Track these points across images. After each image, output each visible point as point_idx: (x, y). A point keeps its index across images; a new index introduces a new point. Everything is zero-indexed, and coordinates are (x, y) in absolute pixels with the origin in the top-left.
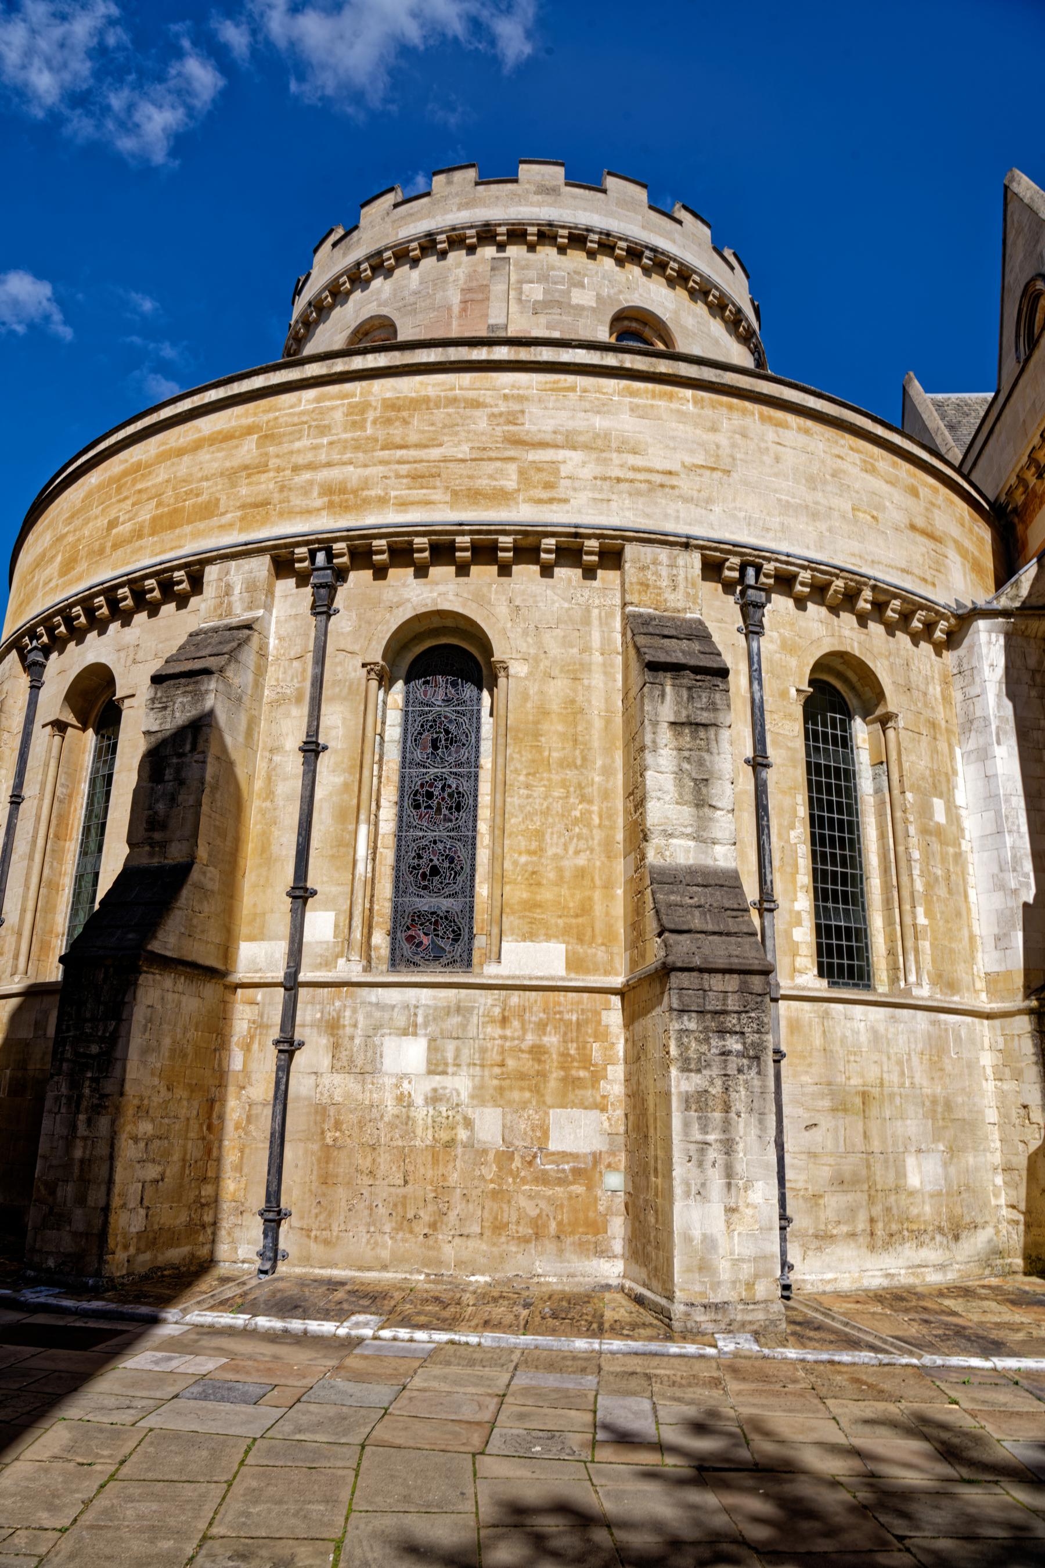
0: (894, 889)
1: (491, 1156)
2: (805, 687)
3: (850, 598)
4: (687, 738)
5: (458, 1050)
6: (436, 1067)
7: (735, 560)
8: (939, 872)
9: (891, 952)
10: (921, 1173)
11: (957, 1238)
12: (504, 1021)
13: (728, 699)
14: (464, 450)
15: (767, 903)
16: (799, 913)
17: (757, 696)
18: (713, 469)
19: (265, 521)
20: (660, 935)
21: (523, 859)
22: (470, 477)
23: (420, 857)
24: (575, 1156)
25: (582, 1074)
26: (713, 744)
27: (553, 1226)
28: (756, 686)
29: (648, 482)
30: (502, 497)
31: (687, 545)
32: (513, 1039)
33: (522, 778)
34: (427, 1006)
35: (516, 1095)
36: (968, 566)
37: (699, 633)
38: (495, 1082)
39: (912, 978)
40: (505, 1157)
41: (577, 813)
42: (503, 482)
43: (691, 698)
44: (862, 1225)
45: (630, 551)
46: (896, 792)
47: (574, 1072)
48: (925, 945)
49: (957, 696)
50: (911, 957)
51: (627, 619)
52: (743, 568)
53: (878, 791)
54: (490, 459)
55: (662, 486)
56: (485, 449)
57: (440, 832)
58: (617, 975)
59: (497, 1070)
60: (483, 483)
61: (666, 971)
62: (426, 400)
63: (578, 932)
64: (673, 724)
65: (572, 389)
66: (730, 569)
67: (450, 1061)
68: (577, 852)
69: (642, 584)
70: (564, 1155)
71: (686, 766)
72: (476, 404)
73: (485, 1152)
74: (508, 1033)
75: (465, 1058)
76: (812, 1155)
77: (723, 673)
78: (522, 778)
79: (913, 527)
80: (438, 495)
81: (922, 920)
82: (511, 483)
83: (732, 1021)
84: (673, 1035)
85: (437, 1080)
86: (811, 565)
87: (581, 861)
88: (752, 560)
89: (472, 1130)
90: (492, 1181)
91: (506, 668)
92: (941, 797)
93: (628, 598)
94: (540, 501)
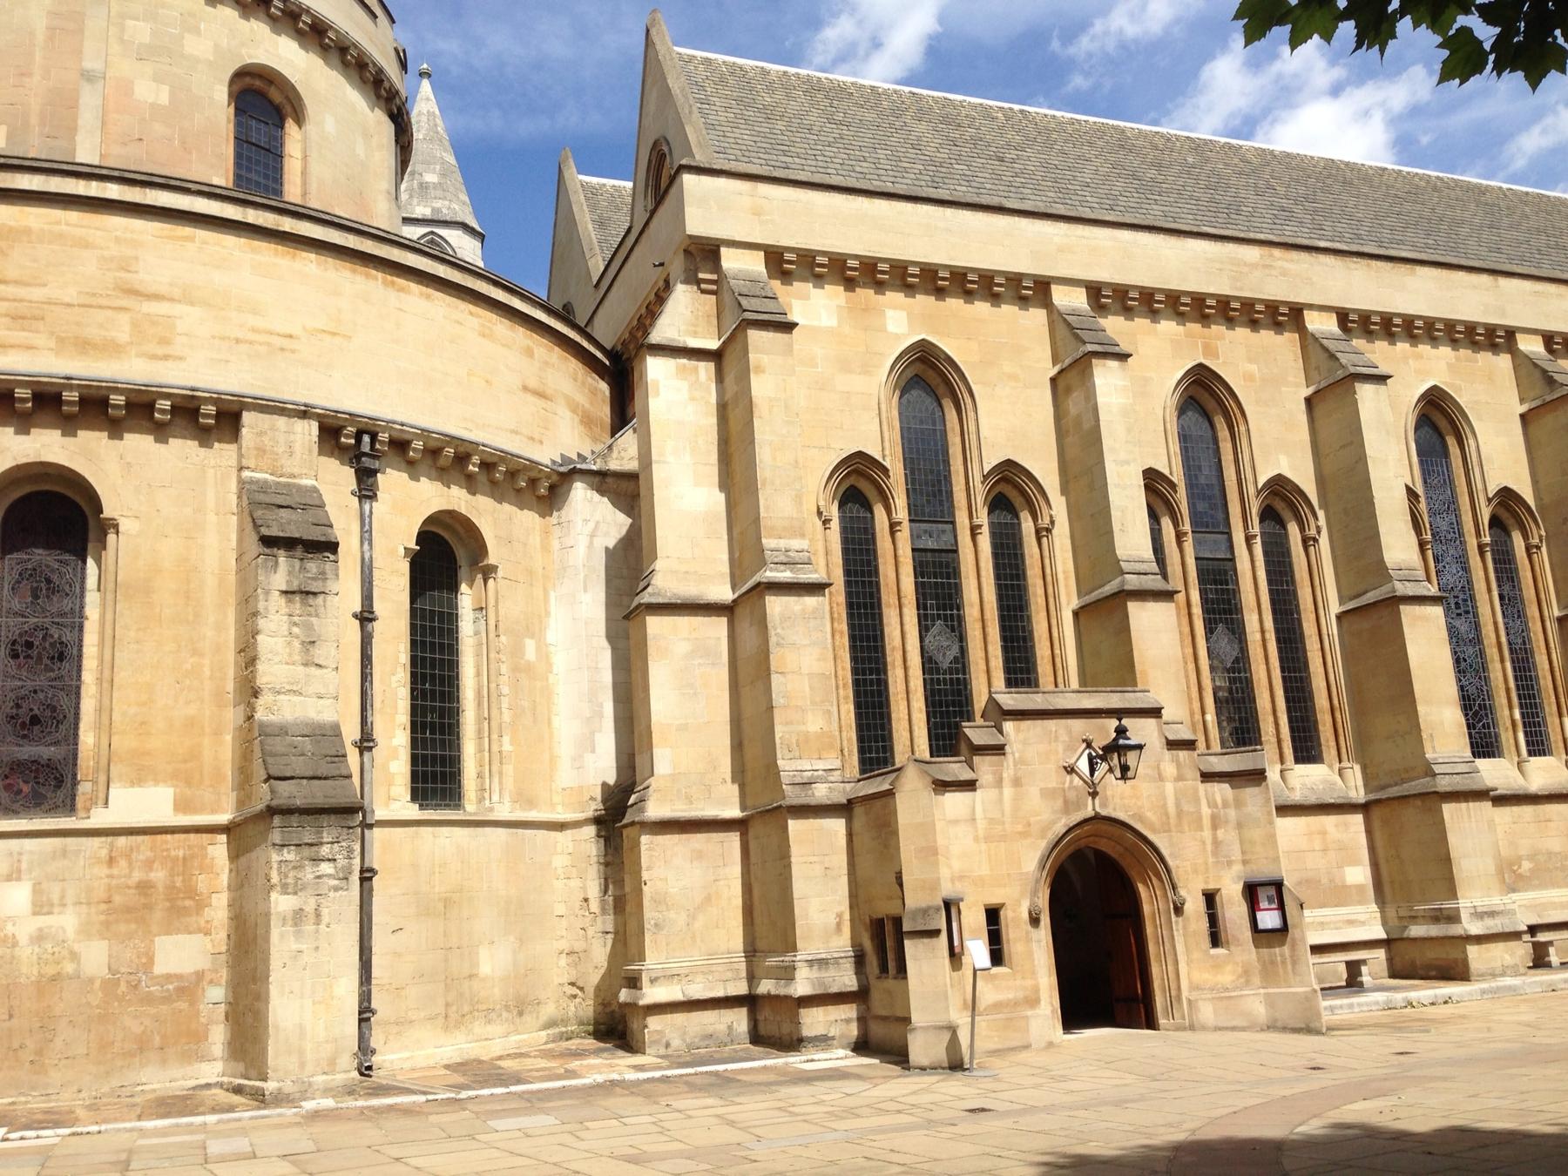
0: (485, 719)
1: (97, 984)
2: (413, 545)
3: (462, 459)
4: (297, 606)
5: (63, 891)
6: (41, 906)
8: (526, 704)
9: (480, 776)
10: (493, 962)
11: (521, 1014)
12: (111, 861)
13: (337, 569)
14: (70, 295)
15: (366, 743)
16: (396, 749)
17: (367, 556)
18: (334, 334)
20: (266, 781)
21: (132, 711)
22: (78, 324)
23: (18, 706)
24: (179, 977)
25: (188, 903)
26: (322, 610)
27: (157, 1040)
28: (366, 546)
29: (269, 344)
30: (112, 349)
31: (304, 413)
32: (119, 877)
33: (132, 634)
34: (31, 852)
35: (123, 928)
36: (577, 419)
37: (312, 503)
38: (103, 917)
39: (495, 798)
40: (109, 986)
41: (188, 666)
42: (114, 334)
43: (303, 569)
44: (441, 1009)
45: (247, 417)
46: (492, 635)
47: (180, 903)
48: (509, 769)
49: (555, 544)
50: (496, 780)
51: (241, 482)
52: (358, 436)
53: (477, 633)
54: (100, 307)
55: (282, 349)
56: (94, 295)
57: (41, 681)
58: (224, 812)
59: (103, 907)
60: (92, 332)
61: (272, 811)
62: (28, 231)
63: (184, 775)
64: (285, 592)
65: (191, 239)
66: (347, 436)
67: (56, 901)
68: (188, 702)
69: (258, 449)
70: (169, 978)
71: (296, 630)
72: (86, 245)
73: (91, 980)
74: (115, 871)
75: (69, 900)
76: (397, 954)
77: (333, 547)
78: (132, 634)
79: (525, 388)
80: (40, 340)
81: (507, 747)
82: (123, 334)
83: (325, 850)
84: (275, 866)
85: (42, 921)
86: (425, 433)
87: (192, 710)
88: (367, 429)
89: (79, 963)
90: (98, 1007)
91: (116, 527)
92: (532, 637)
93: (245, 462)
94: (154, 357)
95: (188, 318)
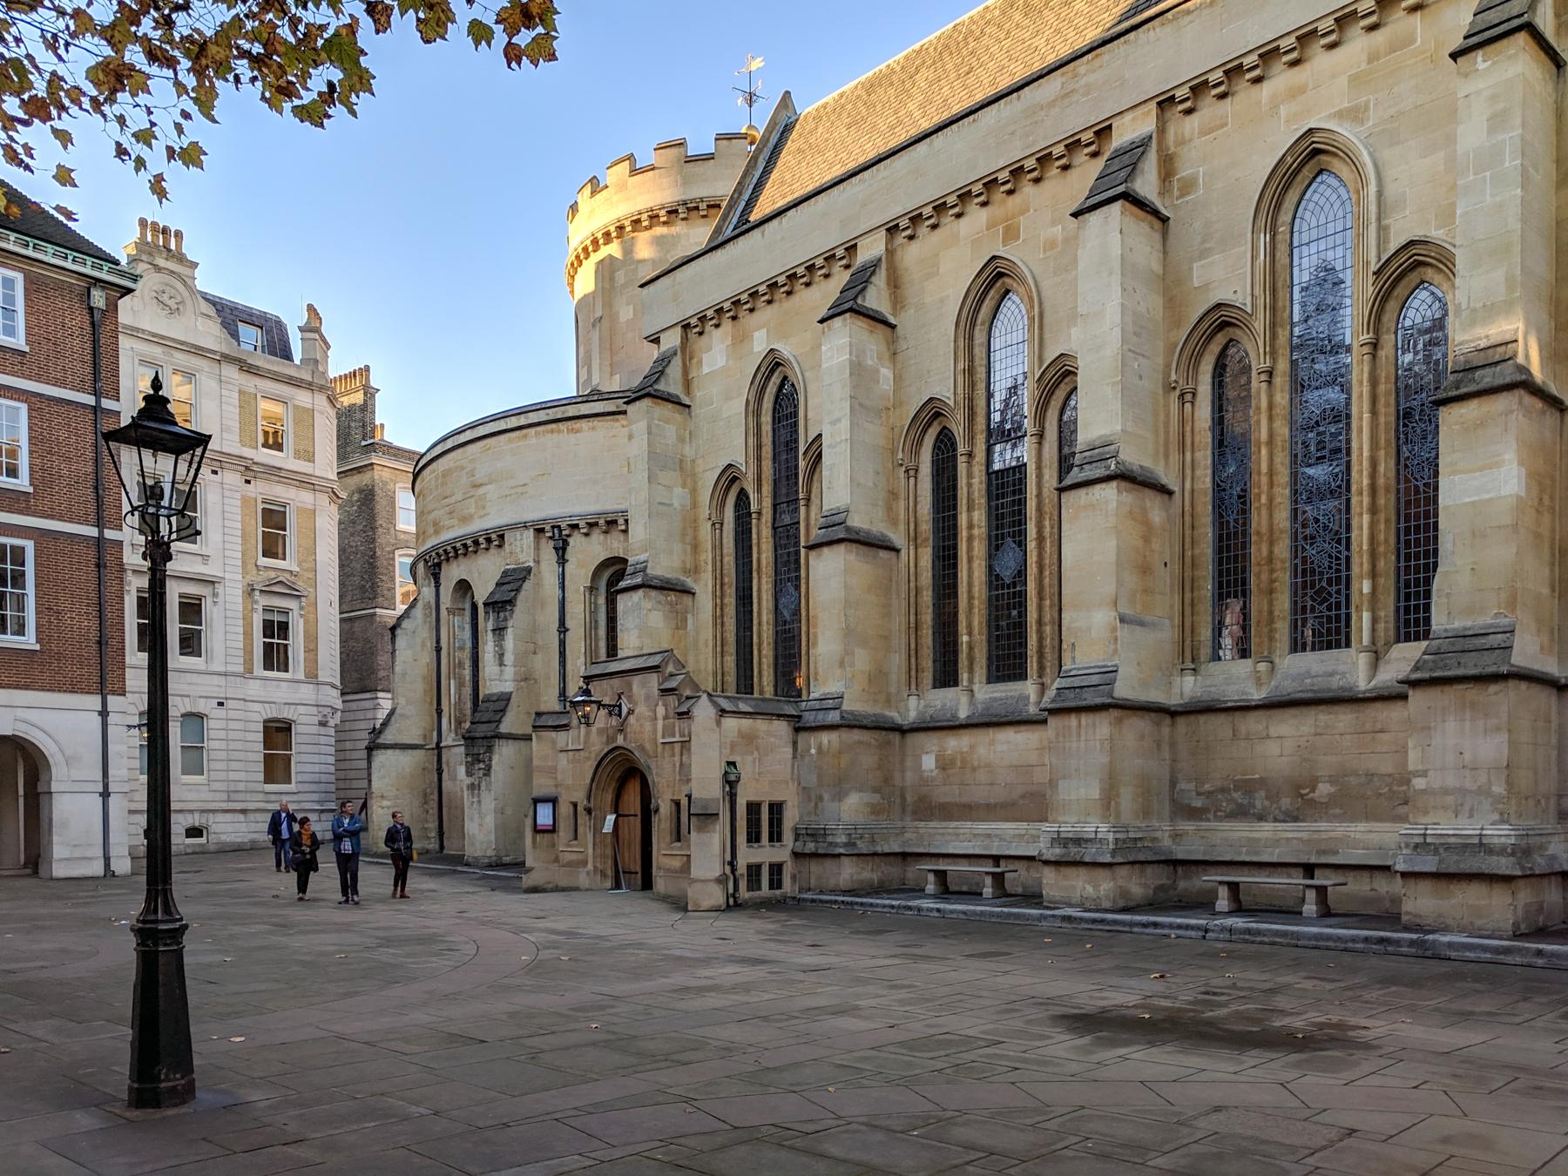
7: (548, 528)
14: (458, 496)
19: (424, 541)
72: (462, 468)
80: (455, 522)
82: (472, 511)
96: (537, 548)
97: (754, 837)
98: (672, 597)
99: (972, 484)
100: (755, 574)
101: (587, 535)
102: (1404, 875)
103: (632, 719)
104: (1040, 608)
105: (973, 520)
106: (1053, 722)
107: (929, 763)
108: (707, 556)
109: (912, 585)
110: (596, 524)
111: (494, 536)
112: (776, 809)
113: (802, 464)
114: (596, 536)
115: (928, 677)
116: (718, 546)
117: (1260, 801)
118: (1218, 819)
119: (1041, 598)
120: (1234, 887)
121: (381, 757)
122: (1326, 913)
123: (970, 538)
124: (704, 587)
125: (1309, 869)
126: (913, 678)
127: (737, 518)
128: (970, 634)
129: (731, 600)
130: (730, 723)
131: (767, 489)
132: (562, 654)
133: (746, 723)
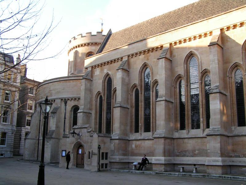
7: (63, 99)
14: (47, 92)
15: (64, 130)
31: (59, 98)
52: (64, 99)
95: (53, 92)
96: (61, 103)
97: (103, 159)
98: (88, 114)
99: (141, 98)
100: (103, 111)
101: (71, 101)
102: (207, 165)
103: (81, 136)
104: (153, 120)
105: (142, 105)
106: (155, 140)
107: (134, 146)
108: (94, 107)
109: (131, 115)
110: (73, 99)
111: (53, 100)
112: (107, 154)
113: (112, 92)
114: (73, 101)
115: (134, 131)
116: (96, 105)
117: (187, 154)
118: (181, 157)
119: (153, 118)
120: (183, 168)
121: (27, 141)
122: (197, 172)
123: (141, 107)
124: (93, 112)
125: (195, 165)
126: (131, 131)
127: (100, 100)
128: (141, 124)
129: (98, 115)
130: (100, 138)
131: (106, 96)
132: (65, 123)
133: (102, 138)
